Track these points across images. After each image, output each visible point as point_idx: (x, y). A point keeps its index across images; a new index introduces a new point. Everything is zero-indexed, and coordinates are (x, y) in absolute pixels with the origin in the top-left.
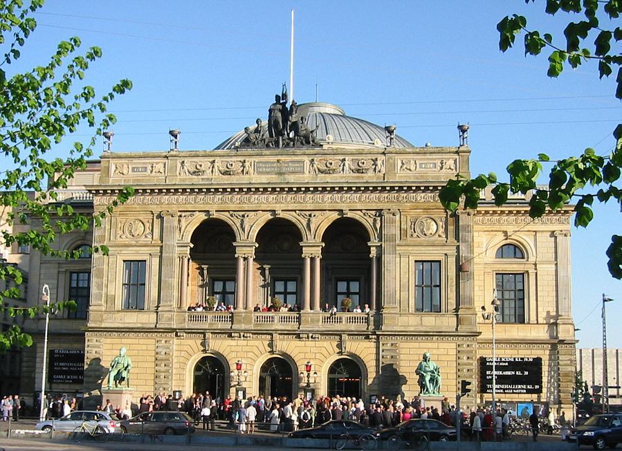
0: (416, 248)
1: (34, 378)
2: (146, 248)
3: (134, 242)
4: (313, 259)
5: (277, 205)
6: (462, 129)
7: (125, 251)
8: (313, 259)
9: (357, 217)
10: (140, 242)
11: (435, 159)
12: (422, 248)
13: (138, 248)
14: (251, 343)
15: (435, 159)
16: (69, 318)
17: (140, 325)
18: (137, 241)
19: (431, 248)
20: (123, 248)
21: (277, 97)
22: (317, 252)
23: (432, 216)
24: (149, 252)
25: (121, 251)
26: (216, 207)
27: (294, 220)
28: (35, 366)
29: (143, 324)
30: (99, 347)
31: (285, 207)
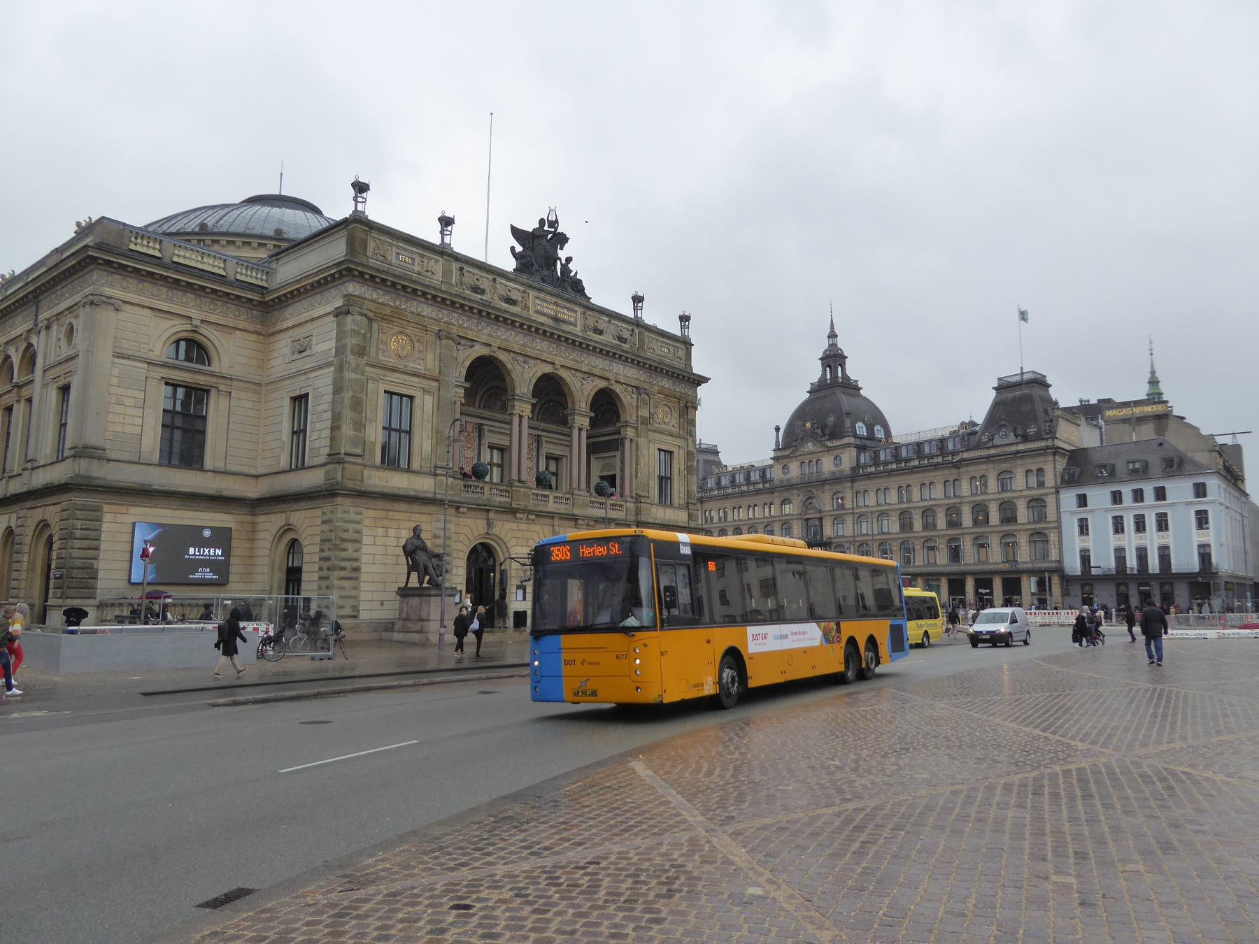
0: (659, 435)
1: (97, 570)
2: (416, 379)
3: (401, 367)
4: (580, 430)
5: (558, 358)
6: (684, 319)
7: (392, 377)
8: (580, 430)
9: (618, 391)
10: (410, 369)
11: (670, 345)
12: (664, 437)
13: (407, 377)
14: (532, 527)
15: (670, 345)
16: (160, 465)
17: (412, 493)
18: (405, 366)
19: (669, 438)
20: (388, 373)
21: (542, 222)
22: (585, 422)
23: (669, 404)
24: (423, 386)
25: (384, 376)
26: (497, 343)
27: (568, 380)
28: (97, 549)
29: (416, 491)
30: (359, 523)
31: (560, 360)
